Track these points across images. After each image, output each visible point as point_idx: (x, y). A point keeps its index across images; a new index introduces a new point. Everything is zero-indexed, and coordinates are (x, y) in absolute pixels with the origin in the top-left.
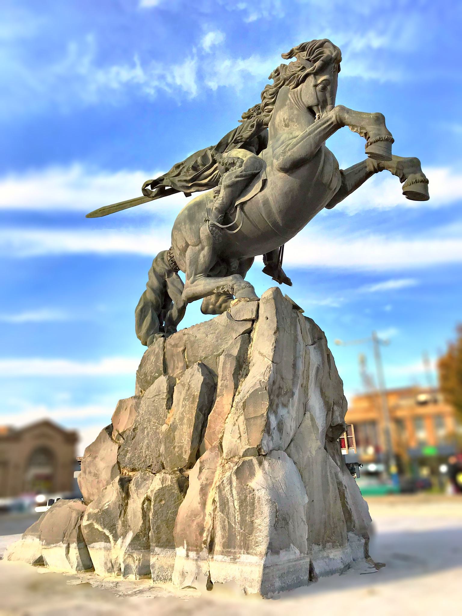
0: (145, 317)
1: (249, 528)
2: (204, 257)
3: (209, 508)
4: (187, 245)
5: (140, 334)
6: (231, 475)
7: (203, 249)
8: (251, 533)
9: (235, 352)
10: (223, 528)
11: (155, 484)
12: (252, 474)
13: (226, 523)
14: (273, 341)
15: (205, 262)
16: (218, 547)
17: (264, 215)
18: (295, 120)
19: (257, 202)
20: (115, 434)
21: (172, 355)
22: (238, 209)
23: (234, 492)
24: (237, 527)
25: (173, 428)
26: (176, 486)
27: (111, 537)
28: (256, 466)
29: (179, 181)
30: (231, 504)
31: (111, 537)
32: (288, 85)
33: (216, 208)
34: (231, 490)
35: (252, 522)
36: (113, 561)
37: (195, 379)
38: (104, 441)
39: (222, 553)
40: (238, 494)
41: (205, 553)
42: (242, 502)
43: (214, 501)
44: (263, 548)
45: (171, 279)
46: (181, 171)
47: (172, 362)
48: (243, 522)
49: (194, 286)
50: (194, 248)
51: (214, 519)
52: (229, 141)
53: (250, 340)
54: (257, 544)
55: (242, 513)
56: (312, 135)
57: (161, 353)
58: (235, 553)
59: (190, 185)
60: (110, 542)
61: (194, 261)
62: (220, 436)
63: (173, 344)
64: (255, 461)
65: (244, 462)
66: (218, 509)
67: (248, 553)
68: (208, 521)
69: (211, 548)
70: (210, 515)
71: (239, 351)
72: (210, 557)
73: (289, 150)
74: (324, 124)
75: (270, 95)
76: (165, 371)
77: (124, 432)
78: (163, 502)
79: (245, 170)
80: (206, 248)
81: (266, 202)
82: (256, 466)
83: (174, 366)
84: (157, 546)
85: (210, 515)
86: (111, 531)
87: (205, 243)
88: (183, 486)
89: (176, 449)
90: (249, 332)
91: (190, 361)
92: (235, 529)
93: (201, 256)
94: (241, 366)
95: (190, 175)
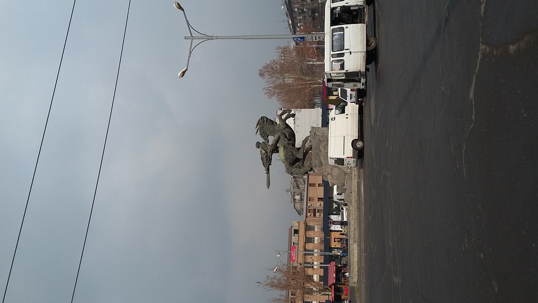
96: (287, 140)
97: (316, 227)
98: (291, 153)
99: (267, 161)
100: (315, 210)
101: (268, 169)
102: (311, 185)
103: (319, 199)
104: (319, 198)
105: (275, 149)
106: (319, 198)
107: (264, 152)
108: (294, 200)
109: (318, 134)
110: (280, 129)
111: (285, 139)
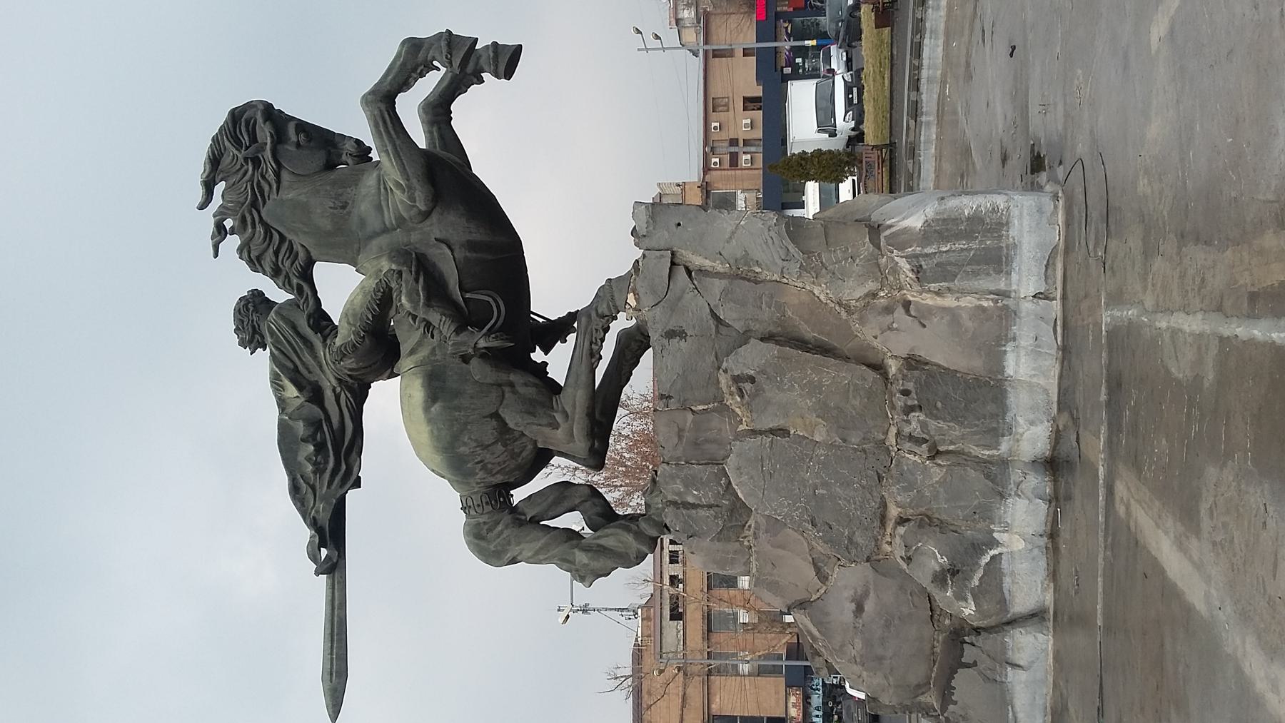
0: (599, 546)
1: (976, 219)
2: (526, 385)
3: (949, 301)
4: (496, 416)
5: (633, 556)
6: (906, 257)
7: (511, 385)
8: (982, 221)
9: (718, 285)
10: (976, 274)
12: (906, 230)
13: (969, 269)
14: (716, 212)
15: (536, 385)
16: (1002, 286)
17: (490, 257)
18: (340, 191)
19: (466, 258)
21: (696, 444)
22: (468, 295)
23: (929, 250)
24: (975, 245)
25: (824, 411)
26: (916, 373)
27: (992, 552)
28: (893, 230)
29: (329, 487)
30: (944, 258)
31: (992, 552)
32: (264, 203)
33: (458, 331)
34: (927, 255)
35: (968, 219)
36: (1030, 547)
37: (753, 357)
38: (827, 614)
39: (1009, 274)
41: (1010, 302)
42: (943, 236)
43: (938, 293)
44: (1000, 201)
45: (526, 510)
46: (308, 484)
47: (707, 446)
48: (968, 235)
49: (574, 413)
50: (505, 402)
51: (964, 293)
52: (290, 365)
53: (702, 272)
54: (995, 210)
55: (958, 236)
56: (398, 142)
58: (1007, 246)
59: (344, 467)
60: (1001, 554)
62: (844, 315)
63: (676, 440)
64: (888, 232)
66: (951, 285)
67: (1007, 223)
68: (968, 302)
69: (1004, 294)
70: (957, 299)
72: (1013, 295)
74: (385, 122)
75: (265, 239)
77: (815, 564)
78: (939, 405)
80: (512, 377)
81: (472, 246)
82: (893, 230)
83: (715, 441)
84: (1004, 419)
85: (957, 299)
86: (983, 553)
87: (503, 377)
89: (856, 403)
91: (715, 399)
92: (976, 249)
93: (522, 390)
94: (742, 274)
95: (327, 462)
96: (445, 326)
97: (741, 196)
98: (488, 431)
99: (323, 458)
100: (733, 142)
101: (330, 536)
102: (717, 54)
103: (750, 103)
104: (746, 100)
105: (379, 350)
106: (746, 100)
107: (291, 391)
108: (678, 21)
109: (697, 261)
110: (390, 218)
111: (435, 317)
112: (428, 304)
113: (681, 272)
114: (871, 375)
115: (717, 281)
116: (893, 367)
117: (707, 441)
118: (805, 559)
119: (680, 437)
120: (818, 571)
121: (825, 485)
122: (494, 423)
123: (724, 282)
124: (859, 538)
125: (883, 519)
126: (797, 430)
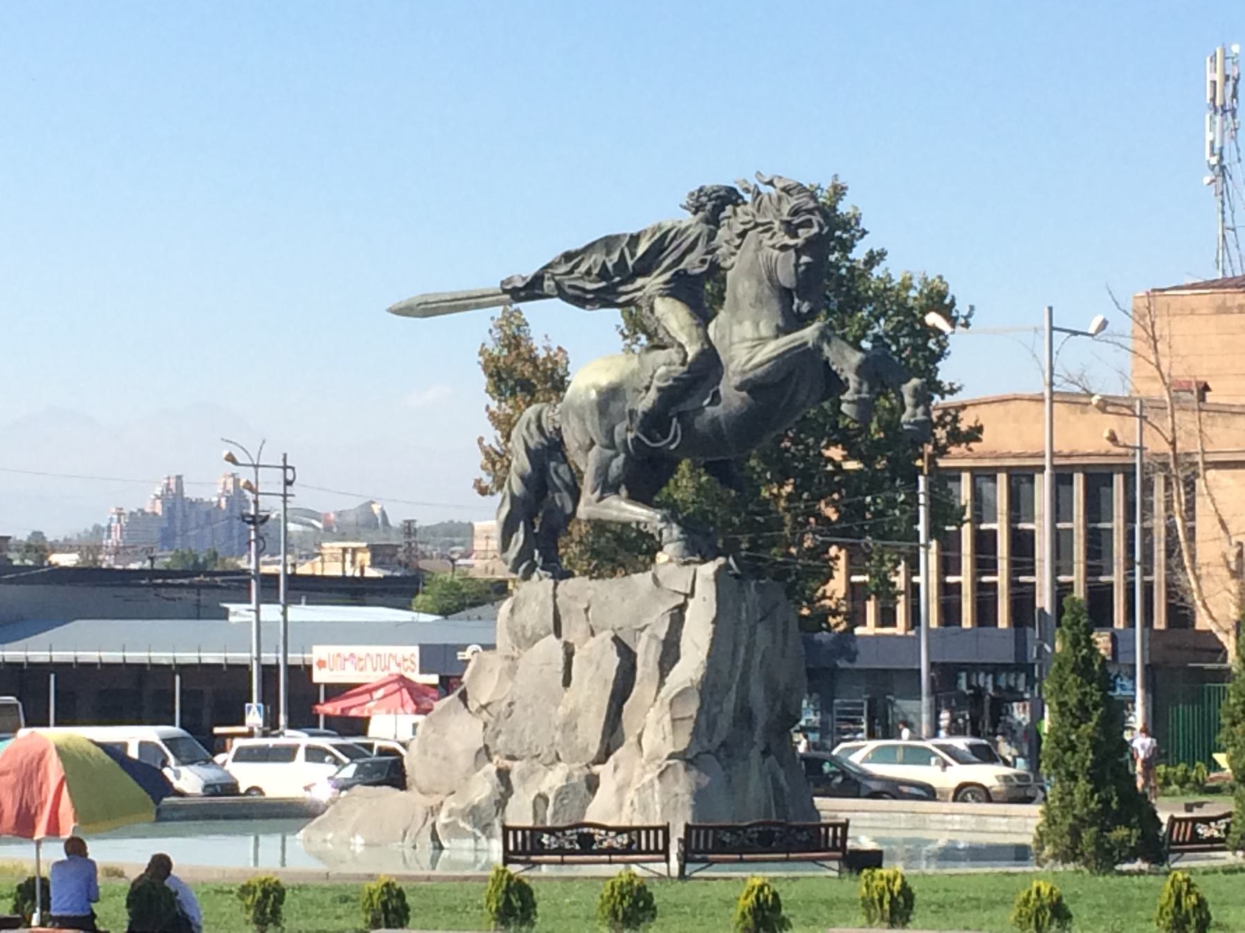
4: (592, 443)
7: (617, 455)
11: (553, 780)
20: (473, 705)
23: (656, 796)
40: (661, 797)
43: (632, 803)
53: (682, 619)
57: (550, 602)
61: (602, 470)
62: (638, 731)
65: (668, 766)
71: (668, 634)
73: (751, 370)
76: (558, 632)
77: (489, 704)
79: (688, 372)
88: (592, 784)
90: (682, 608)
94: (670, 653)
95: (591, 282)
112: (659, 389)
113: (681, 600)
114: (594, 750)
115: (666, 629)
116: (597, 769)
117: (570, 619)
118: (492, 696)
119: (570, 597)
120: (484, 707)
121: (533, 713)
122: (588, 442)
123: (662, 636)
124: (502, 738)
125: (512, 758)
126: (568, 695)
